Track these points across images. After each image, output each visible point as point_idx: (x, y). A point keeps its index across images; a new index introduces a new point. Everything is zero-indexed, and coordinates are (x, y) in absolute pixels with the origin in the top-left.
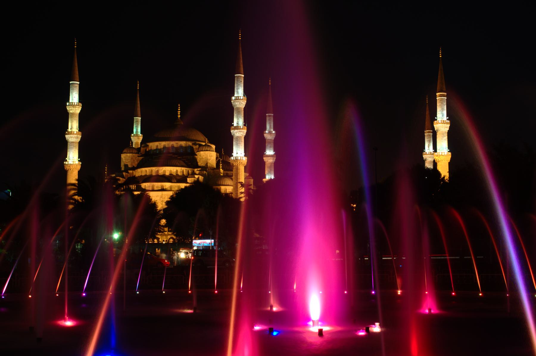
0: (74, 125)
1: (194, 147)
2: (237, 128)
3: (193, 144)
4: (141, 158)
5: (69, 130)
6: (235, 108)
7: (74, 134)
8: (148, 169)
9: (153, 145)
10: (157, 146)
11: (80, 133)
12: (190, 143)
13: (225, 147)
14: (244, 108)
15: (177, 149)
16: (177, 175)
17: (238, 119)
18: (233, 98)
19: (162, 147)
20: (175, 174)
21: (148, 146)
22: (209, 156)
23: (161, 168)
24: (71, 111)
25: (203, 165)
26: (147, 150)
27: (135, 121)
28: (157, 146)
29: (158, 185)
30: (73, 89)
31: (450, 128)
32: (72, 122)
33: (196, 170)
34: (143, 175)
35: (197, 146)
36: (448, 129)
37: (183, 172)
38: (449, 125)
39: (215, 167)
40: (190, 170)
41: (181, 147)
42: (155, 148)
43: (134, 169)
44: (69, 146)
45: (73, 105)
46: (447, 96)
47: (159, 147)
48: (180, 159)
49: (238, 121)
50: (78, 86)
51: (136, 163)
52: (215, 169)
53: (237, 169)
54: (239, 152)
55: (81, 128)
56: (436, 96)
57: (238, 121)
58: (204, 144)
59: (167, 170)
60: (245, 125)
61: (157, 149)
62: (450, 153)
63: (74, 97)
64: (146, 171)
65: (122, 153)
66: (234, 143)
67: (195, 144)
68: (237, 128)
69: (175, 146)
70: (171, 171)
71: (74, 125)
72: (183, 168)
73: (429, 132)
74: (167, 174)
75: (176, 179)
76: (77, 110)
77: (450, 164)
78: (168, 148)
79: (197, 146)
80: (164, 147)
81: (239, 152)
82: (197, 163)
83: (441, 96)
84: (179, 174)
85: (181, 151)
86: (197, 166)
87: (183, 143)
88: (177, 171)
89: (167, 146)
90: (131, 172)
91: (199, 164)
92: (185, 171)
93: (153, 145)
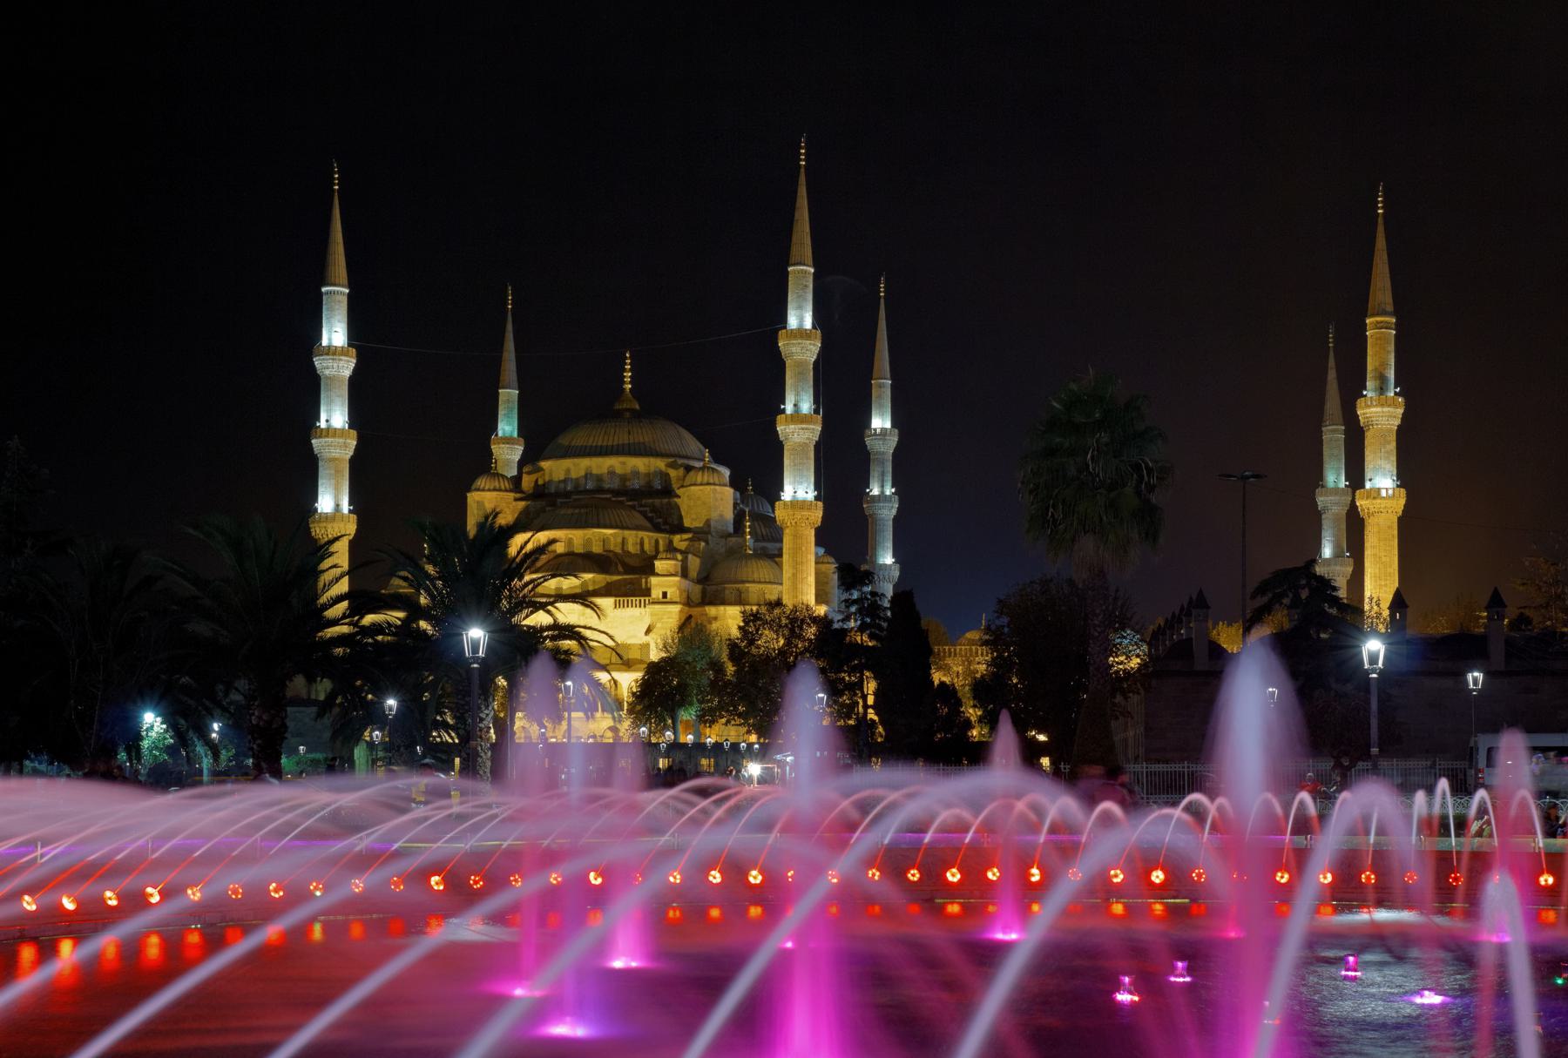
0: (335, 415)
1: (673, 473)
2: (797, 417)
3: (670, 465)
5: (323, 424)
6: (788, 363)
7: (334, 436)
9: (555, 469)
10: (568, 471)
11: (354, 433)
12: (659, 464)
13: (758, 473)
14: (816, 363)
15: (624, 478)
17: (797, 394)
18: (782, 333)
19: (582, 473)
20: (618, 550)
21: (540, 469)
22: (710, 498)
24: (327, 372)
25: (699, 524)
26: (540, 482)
27: (501, 399)
28: (568, 471)
30: (331, 310)
31: (1405, 417)
32: (330, 403)
33: (677, 538)
35: (681, 471)
36: (1398, 422)
37: (642, 544)
38: (1401, 411)
39: (731, 530)
40: (662, 538)
41: (636, 473)
44: (322, 472)
45: (331, 351)
46: (1398, 326)
47: (574, 475)
48: (633, 507)
49: (799, 400)
50: (345, 300)
52: (730, 535)
53: (796, 536)
54: (798, 488)
55: (355, 420)
56: (1364, 327)
57: (799, 400)
58: (698, 464)
60: (816, 411)
61: (565, 481)
62: (1403, 491)
63: (335, 333)
65: (469, 490)
66: (786, 462)
68: (797, 417)
69: (619, 470)
70: (605, 541)
71: (335, 415)
72: (641, 534)
73: (1334, 431)
74: (597, 549)
75: (624, 564)
76: (345, 368)
77: (1399, 519)
78: (599, 478)
80: (588, 475)
81: (798, 488)
82: (681, 518)
83: (1378, 326)
84: (631, 548)
85: (636, 484)
86: (681, 529)
87: (640, 464)
88: (624, 541)
89: (595, 472)
91: (687, 523)
92: (646, 541)
93: (555, 469)
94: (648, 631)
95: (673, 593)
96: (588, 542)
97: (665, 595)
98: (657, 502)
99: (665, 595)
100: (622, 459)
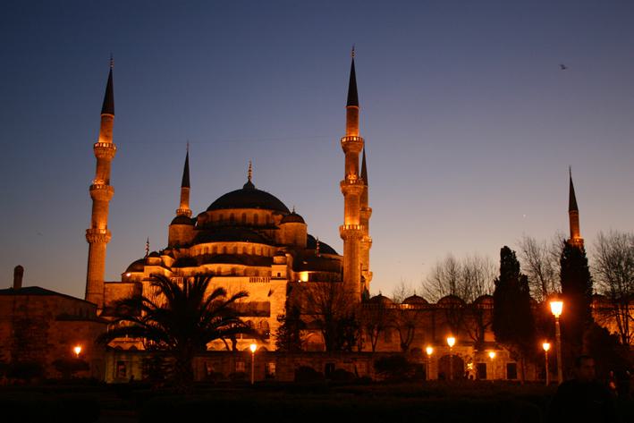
3: (273, 214)
4: (197, 231)
8: (210, 245)
10: (221, 216)
12: (268, 213)
16: (254, 255)
20: (250, 253)
23: (231, 243)
29: (226, 267)
34: (203, 253)
42: (218, 219)
43: (188, 245)
47: (224, 218)
51: (191, 239)
59: (241, 246)
61: (221, 220)
64: (207, 248)
67: (276, 214)
72: (262, 245)
74: (240, 252)
79: (280, 217)
80: (232, 217)
84: (258, 253)
88: (254, 249)
90: (183, 250)
94: (270, 294)
95: (283, 274)
96: (236, 248)
97: (279, 274)
98: (268, 231)
99: (279, 274)
100: (249, 210)
